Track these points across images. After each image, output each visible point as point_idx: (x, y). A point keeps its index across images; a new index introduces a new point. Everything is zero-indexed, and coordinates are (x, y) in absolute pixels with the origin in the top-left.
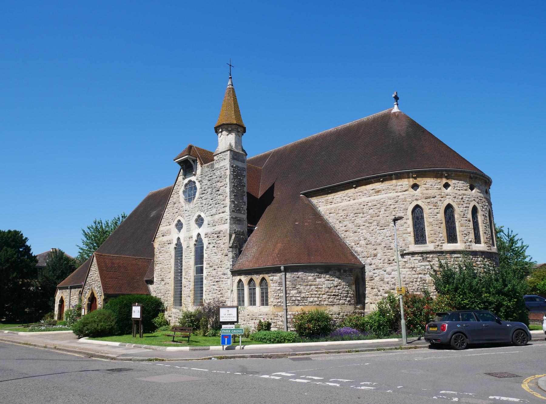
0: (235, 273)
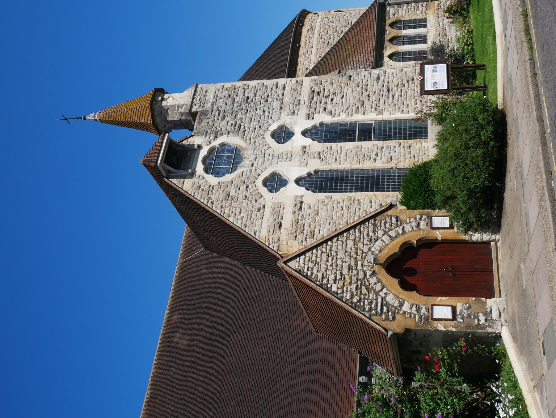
0: (378, 63)
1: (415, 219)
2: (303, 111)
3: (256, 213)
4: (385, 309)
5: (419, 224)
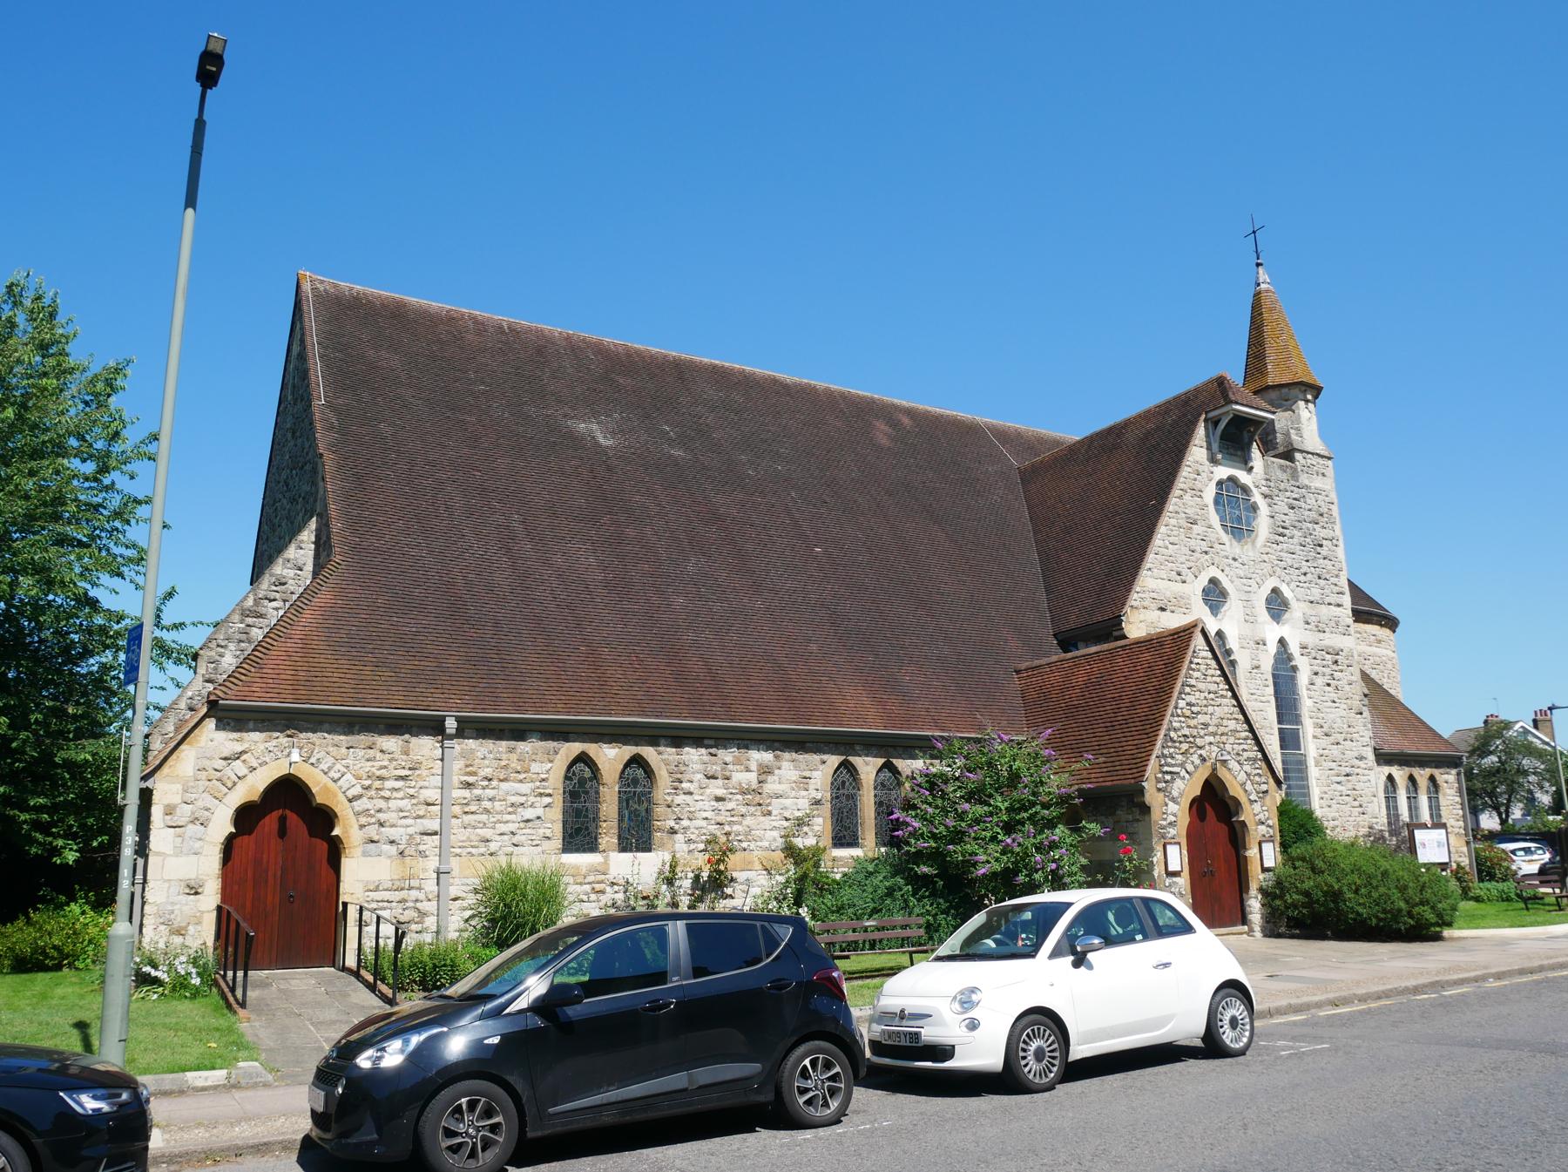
0: (1383, 758)
1: (1268, 819)
2: (1312, 639)
3: (1175, 569)
4: (1168, 777)
5: (1263, 823)
